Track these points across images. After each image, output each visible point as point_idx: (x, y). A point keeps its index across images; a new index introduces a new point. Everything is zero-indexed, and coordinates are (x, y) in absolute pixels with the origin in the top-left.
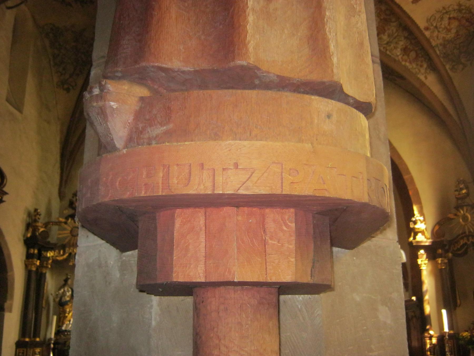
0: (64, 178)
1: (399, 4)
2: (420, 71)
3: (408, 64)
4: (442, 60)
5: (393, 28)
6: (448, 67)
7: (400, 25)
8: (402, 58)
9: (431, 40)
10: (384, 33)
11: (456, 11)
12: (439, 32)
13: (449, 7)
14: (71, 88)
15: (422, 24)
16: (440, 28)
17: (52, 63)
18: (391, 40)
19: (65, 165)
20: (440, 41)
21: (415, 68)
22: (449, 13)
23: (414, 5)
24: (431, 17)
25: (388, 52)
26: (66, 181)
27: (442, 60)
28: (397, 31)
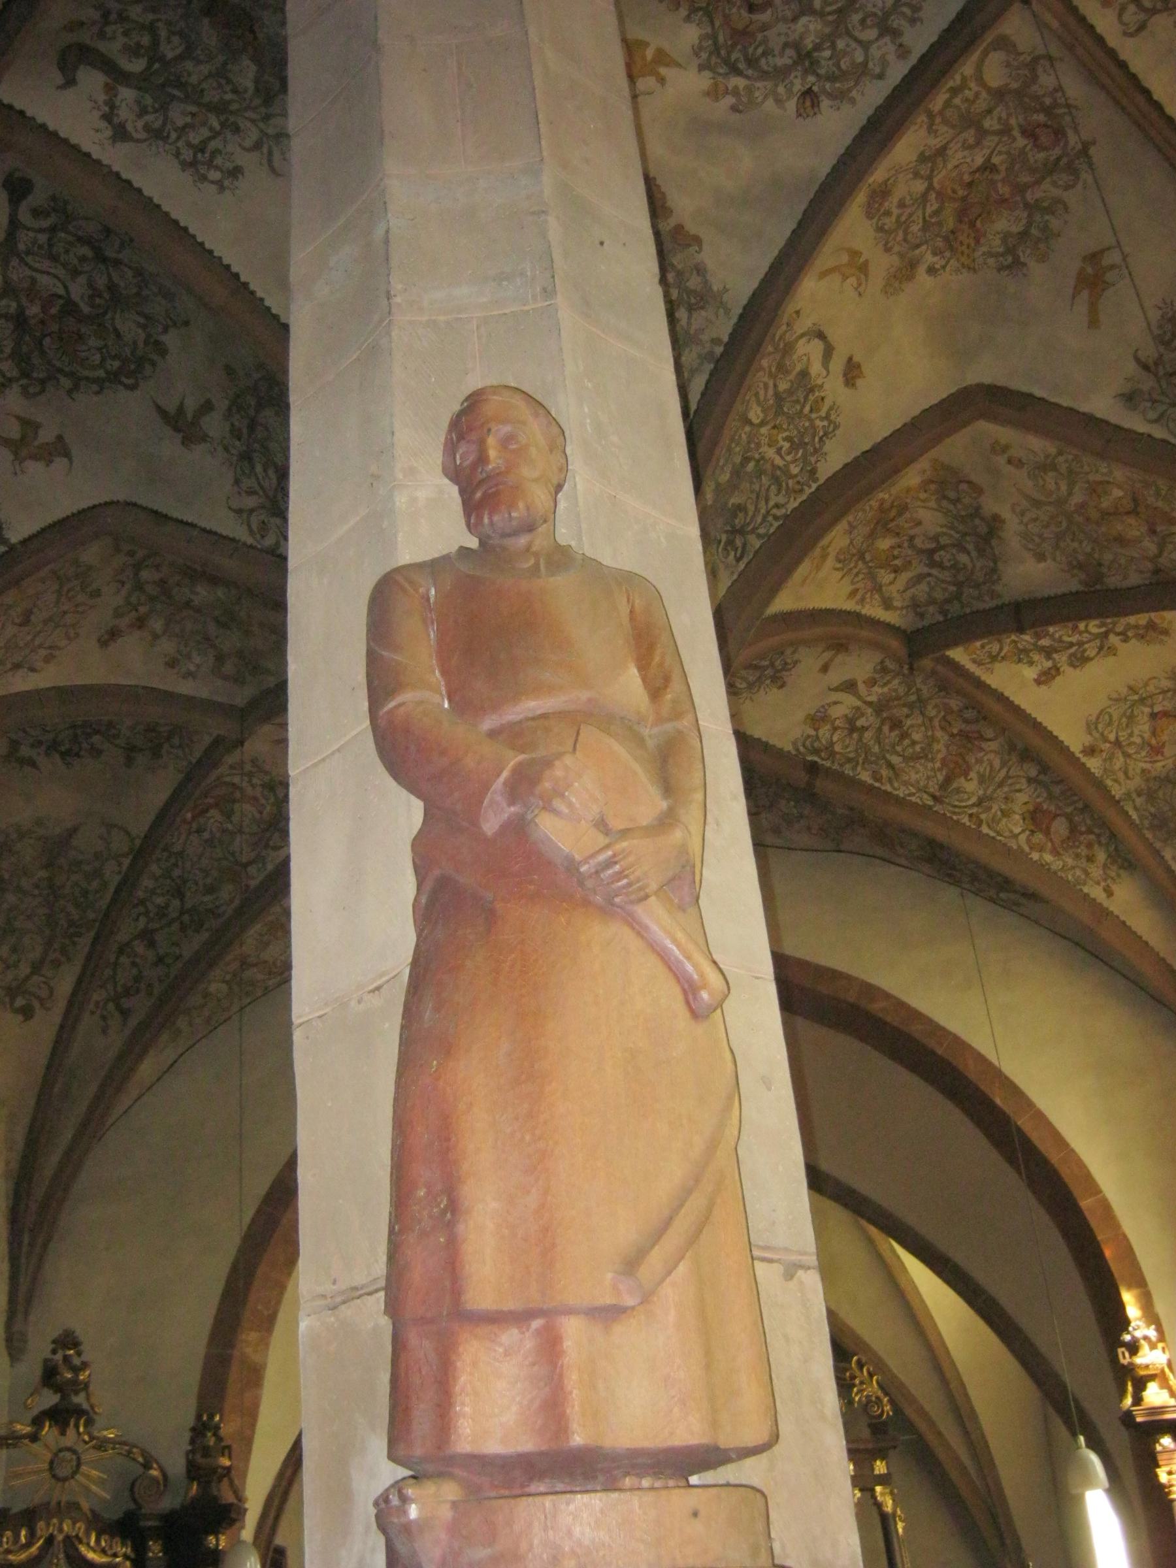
0: (23, 1289)
1: (1000, 690)
2: (1087, 873)
3: (1048, 857)
4: (1149, 835)
5: (991, 756)
7: (1012, 747)
8: (1028, 840)
9: (1109, 783)
10: (966, 774)
11: (1169, 694)
12: (1127, 755)
13: (1146, 685)
14: (36, 1004)
15: (1074, 739)
16: (1129, 745)
18: (989, 792)
19: (25, 1249)
20: (1137, 782)
21: (1073, 868)
22: (1149, 702)
23: (1044, 687)
24: (1098, 718)
25: (985, 829)
26: (29, 1301)
27: (1149, 835)
28: (1004, 764)
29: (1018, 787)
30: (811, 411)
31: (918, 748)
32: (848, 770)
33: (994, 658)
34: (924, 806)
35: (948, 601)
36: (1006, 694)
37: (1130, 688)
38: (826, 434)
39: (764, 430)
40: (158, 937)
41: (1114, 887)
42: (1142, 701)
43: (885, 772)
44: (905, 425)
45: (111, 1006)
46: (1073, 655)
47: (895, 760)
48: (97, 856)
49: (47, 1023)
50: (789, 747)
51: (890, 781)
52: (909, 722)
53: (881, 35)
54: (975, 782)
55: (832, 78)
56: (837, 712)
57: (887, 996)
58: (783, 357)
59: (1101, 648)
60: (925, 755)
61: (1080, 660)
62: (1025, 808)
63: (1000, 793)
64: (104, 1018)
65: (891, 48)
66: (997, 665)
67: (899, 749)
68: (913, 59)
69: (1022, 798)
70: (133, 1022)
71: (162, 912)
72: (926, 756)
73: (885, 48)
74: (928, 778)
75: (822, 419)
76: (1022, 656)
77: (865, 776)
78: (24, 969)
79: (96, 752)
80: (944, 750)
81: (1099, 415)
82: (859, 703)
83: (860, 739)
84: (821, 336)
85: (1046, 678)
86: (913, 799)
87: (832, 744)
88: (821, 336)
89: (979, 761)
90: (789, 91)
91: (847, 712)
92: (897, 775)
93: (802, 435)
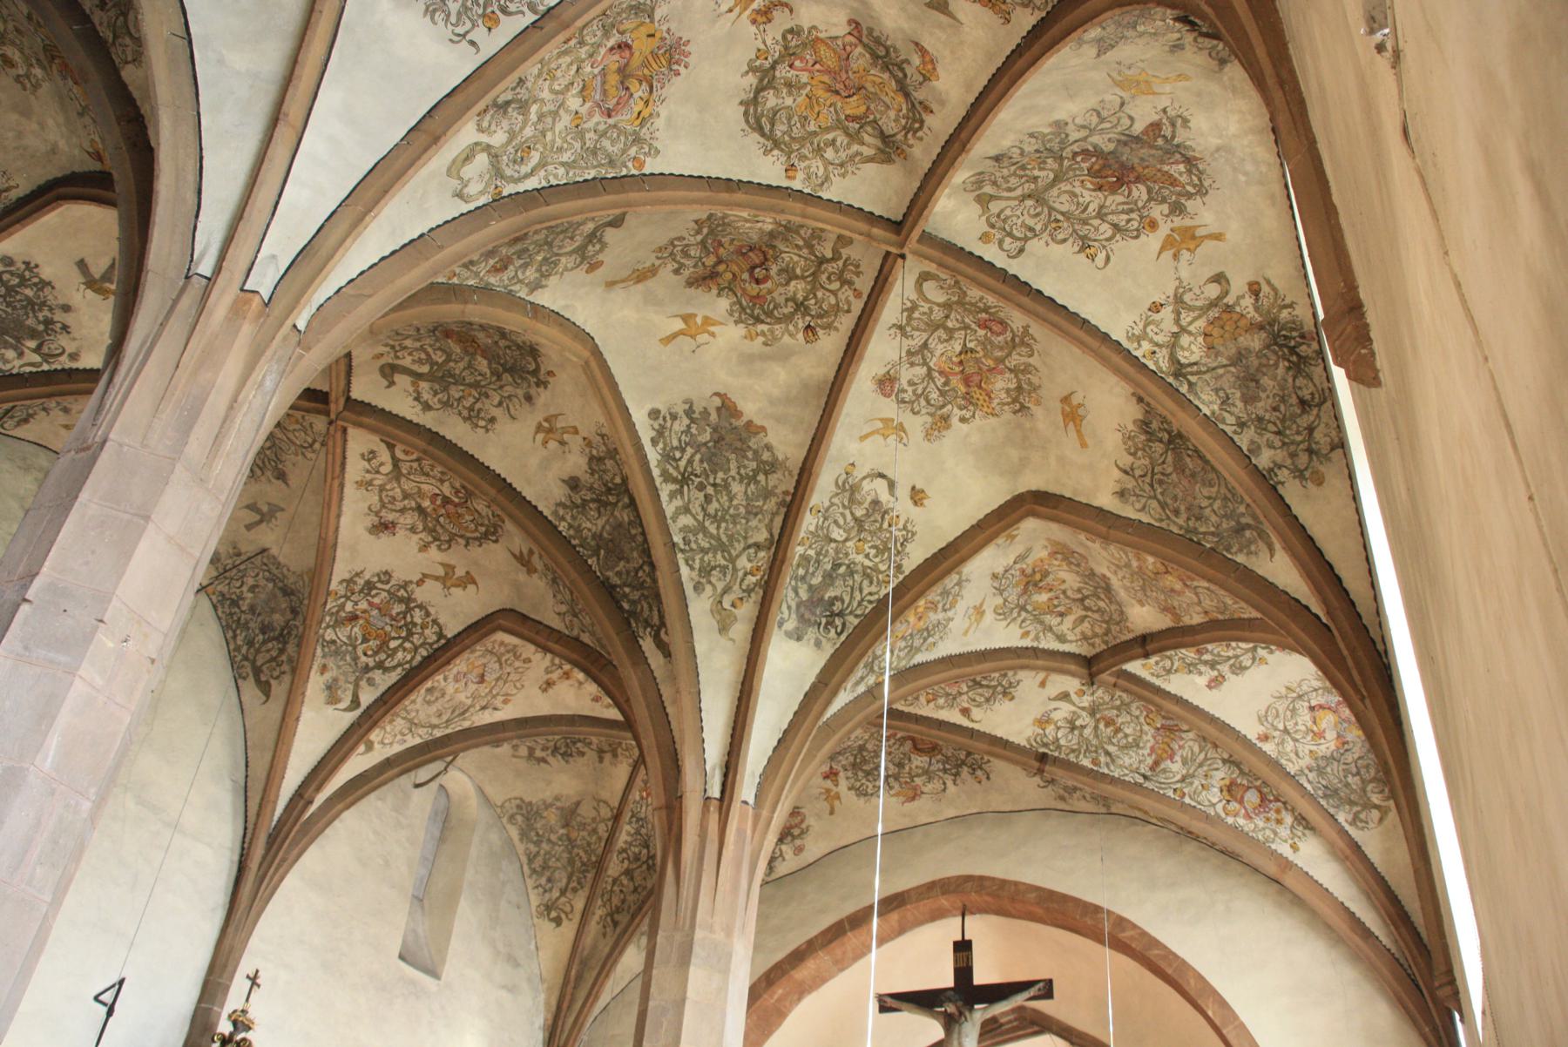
2: (1275, 833)
3: (1241, 821)
4: (1323, 802)
5: (1191, 743)
6: (1342, 817)
8: (1224, 808)
9: (1283, 762)
10: (1171, 758)
11: (1320, 692)
12: (1295, 740)
13: (1300, 686)
14: (563, 916)
15: (1251, 730)
16: (1296, 731)
17: (526, 868)
20: (1307, 761)
25: (1187, 800)
29: (1215, 766)
30: (890, 525)
31: (1130, 739)
32: (1072, 758)
33: (1169, 672)
34: (1136, 783)
35: (1106, 634)
36: (1185, 697)
37: (1288, 688)
38: (906, 540)
39: (849, 544)
40: (636, 873)
41: (1300, 844)
42: (1300, 697)
43: (1103, 759)
44: (973, 526)
45: (609, 919)
46: (1231, 666)
47: (1111, 749)
48: (594, 820)
49: (569, 929)
50: (1024, 743)
51: (1107, 765)
52: (1120, 720)
53: (841, 286)
54: (1180, 763)
55: (820, 316)
56: (1056, 716)
57: (1134, 926)
58: (852, 493)
59: (1254, 659)
60: (1136, 745)
61: (1239, 669)
62: (1222, 783)
63: (1201, 771)
64: (604, 927)
65: (850, 293)
66: (1172, 676)
67: (1115, 741)
68: (865, 297)
69: (1219, 775)
70: (619, 930)
71: (637, 858)
72: (1138, 746)
73: (845, 293)
74: (1140, 762)
75: (900, 530)
76: (1190, 668)
77: (1086, 763)
78: (556, 894)
79: (582, 754)
80: (1152, 741)
81: (1106, 508)
82: (1073, 708)
83: (1081, 735)
84: (882, 476)
85: (1215, 683)
86: (1127, 779)
87: (1058, 740)
88: (882, 476)
89: (1181, 747)
90: (796, 326)
91: (1066, 715)
92: (1113, 761)
93: (885, 543)
